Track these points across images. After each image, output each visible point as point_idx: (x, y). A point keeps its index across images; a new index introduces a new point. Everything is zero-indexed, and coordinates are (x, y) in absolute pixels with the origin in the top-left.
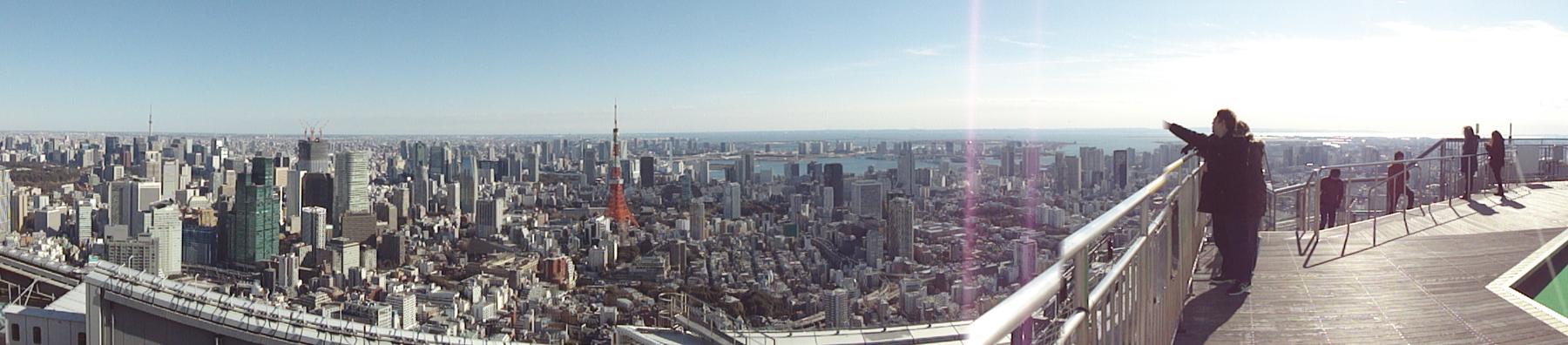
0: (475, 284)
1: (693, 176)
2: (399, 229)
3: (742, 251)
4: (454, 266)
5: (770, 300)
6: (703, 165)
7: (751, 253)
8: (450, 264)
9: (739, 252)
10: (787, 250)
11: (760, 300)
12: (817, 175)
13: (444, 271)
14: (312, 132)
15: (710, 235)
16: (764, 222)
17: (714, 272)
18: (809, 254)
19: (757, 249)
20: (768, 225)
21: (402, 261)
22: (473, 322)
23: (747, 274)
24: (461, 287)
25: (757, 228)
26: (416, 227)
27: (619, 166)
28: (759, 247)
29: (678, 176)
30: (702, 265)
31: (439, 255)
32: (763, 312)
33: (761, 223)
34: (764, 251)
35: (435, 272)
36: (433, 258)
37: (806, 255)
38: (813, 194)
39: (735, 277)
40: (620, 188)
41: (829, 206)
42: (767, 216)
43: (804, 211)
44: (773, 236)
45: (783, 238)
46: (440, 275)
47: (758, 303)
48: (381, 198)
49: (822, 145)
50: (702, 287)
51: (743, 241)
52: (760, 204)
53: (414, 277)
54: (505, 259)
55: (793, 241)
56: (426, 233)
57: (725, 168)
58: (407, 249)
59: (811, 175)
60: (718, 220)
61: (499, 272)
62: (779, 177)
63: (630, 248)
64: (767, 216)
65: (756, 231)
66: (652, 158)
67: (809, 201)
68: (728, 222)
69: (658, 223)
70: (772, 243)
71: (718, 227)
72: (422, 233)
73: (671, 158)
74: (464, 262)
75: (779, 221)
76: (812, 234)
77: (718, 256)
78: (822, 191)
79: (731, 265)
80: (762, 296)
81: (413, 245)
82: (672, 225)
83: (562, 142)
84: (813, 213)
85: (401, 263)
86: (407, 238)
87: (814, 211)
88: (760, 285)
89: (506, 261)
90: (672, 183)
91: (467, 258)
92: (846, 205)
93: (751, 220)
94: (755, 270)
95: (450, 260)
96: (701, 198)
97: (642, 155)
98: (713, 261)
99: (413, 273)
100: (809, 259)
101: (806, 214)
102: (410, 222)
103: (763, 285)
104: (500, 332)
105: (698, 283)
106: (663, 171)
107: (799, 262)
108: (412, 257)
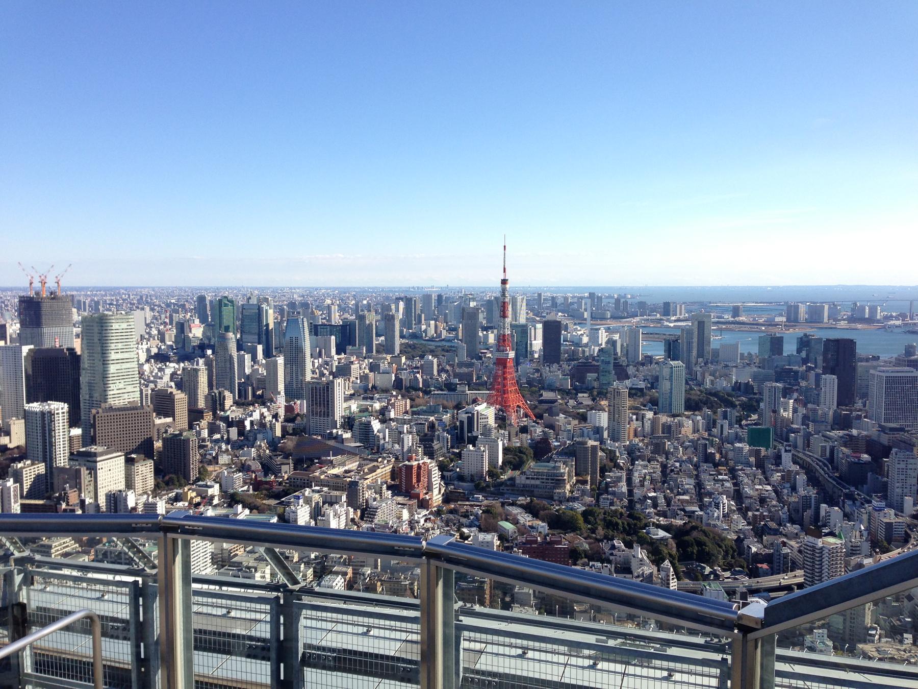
0: (301, 501)
1: (619, 350)
2: (191, 427)
3: (681, 462)
4: (273, 477)
5: (719, 540)
6: (633, 334)
7: (696, 466)
8: (266, 475)
9: (677, 464)
10: (751, 466)
11: (704, 538)
12: (812, 355)
13: (257, 485)
14: (43, 283)
15: (636, 435)
16: (719, 422)
17: (635, 491)
18: (788, 478)
19: (706, 462)
20: (726, 427)
21: (194, 474)
22: (296, 559)
23: (686, 497)
24: (280, 510)
25: (708, 429)
26: (218, 422)
27: (508, 332)
28: (708, 458)
29: (597, 349)
30: (619, 479)
31: (249, 463)
32: (706, 557)
33: (714, 422)
34: (716, 465)
35: (245, 488)
36: (243, 468)
37: (783, 477)
38: (803, 384)
39: (668, 501)
40: (510, 364)
41: (828, 404)
42: (725, 412)
43: (785, 411)
44: (732, 444)
45: (746, 448)
46: (251, 492)
47: (700, 544)
48: (165, 382)
49: (826, 307)
50: (616, 511)
51: (686, 448)
52: (715, 394)
53: (212, 497)
54: (343, 464)
55: (763, 454)
56: (234, 432)
57: (665, 339)
58: (203, 456)
59: (804, 354)
60: (650, 415)
61: (336, 483)
62: (749, 354)
63: (520, 450)
64: (725, 412)
65: (706, 435)
66: (560, 322)
67: (795, 395)
68: (664, 419)
69: (562, 416)
70: (731, 455)
71: (648, 425)
72: (228, 432)
73: (589, 322)
74: (287, 471)
75: (744, 422)
76: (795, 447)
77: (645, 467)
78: (818, 376)
79: (664, 482)
80: (705, 533)
81: (212, 449)
82: (583, 418)
83: (434, 297)
84: (800, 414)
85: (193, 478)
86: (204, 440)
87: (802, 411)
88: (705, 517)
89: (346, 468)
90: (587, 358)
91: (292, 465)
92: (859, 404)
93: (699, 418)
94: (700, 491)
95: (267, 468)
96: (628, 382)
97: (550, 317)
98: (636, 474)
99: (210, 492)
100: (788, 485)
101: (787, 414)
102: (208, 417)
103: (710, 517)
104: (331, 572)
105: (612, 504)
106: (576, 341)
107: (769, 488)
108: (210, 468)
